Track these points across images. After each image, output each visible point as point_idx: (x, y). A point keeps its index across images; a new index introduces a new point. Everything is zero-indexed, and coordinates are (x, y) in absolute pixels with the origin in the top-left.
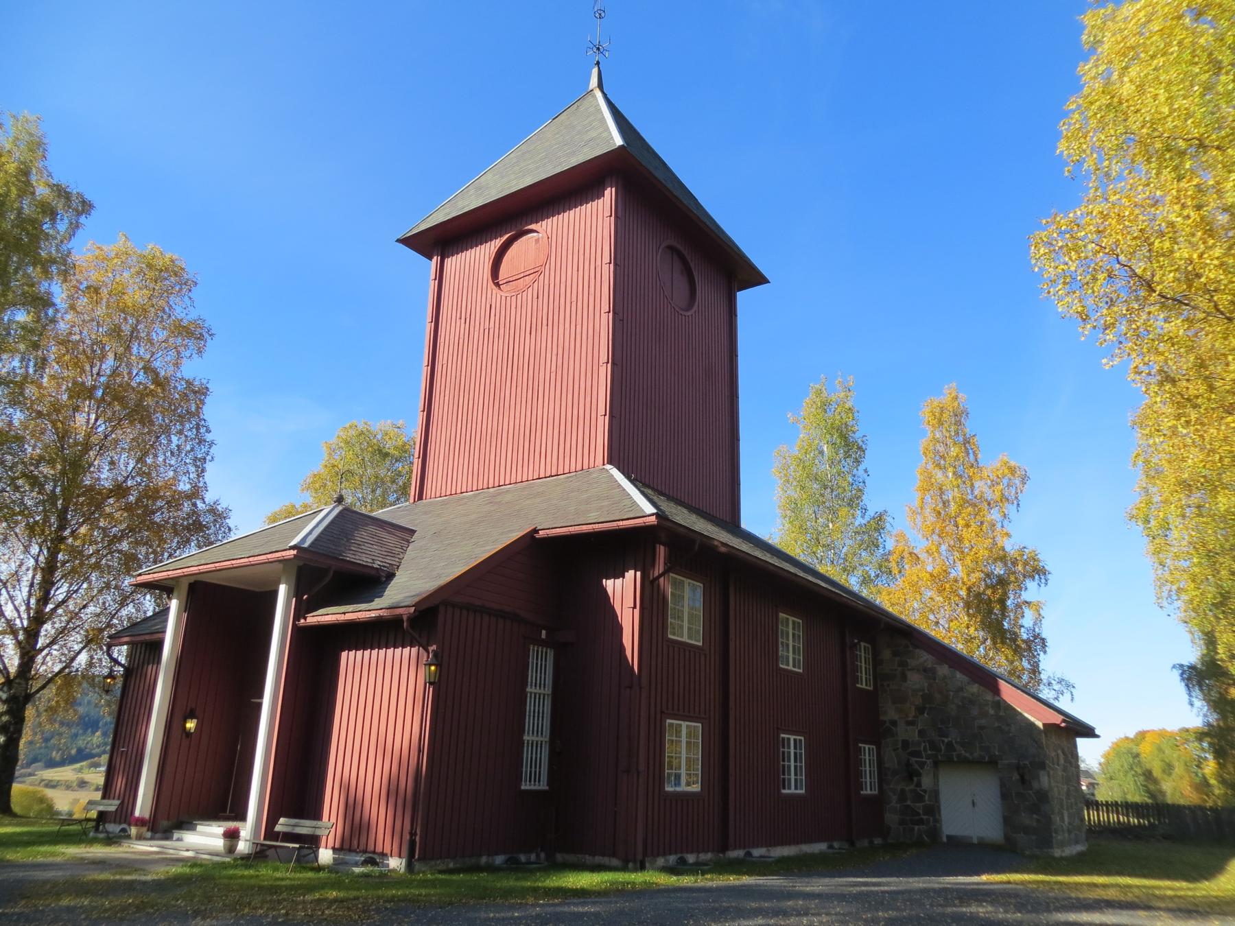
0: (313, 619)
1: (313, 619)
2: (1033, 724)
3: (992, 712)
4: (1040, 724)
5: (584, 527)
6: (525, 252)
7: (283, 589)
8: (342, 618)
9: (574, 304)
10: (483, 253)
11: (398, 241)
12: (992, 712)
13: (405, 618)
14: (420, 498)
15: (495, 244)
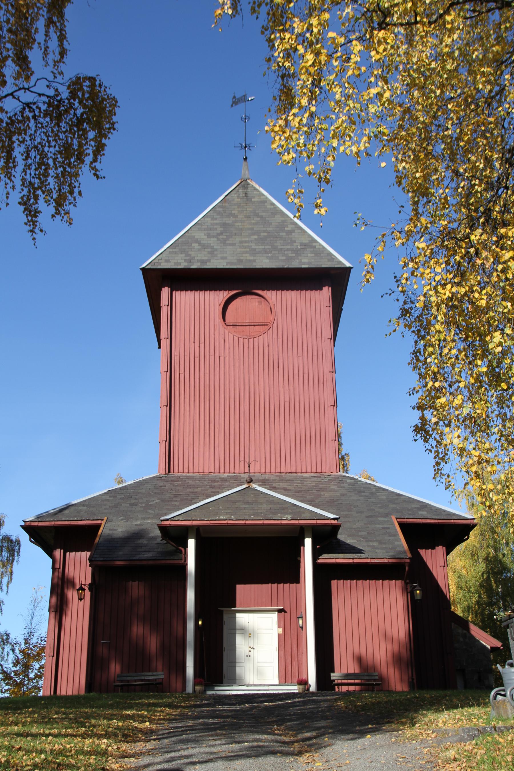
0: (326, 558)
1: (326, 558)
2: (485, 647)
3: (461, 639)
4: (489, 647)
5: (428, 521)
6: (247, 307)
7: (308, 542)
8: (356, 561)
9: (300, 359)
10: (212, 299)
11: (144, 270)
12: (461, 639)
13: (406, 565)
14: (169, 472)
15: (224, 295)
